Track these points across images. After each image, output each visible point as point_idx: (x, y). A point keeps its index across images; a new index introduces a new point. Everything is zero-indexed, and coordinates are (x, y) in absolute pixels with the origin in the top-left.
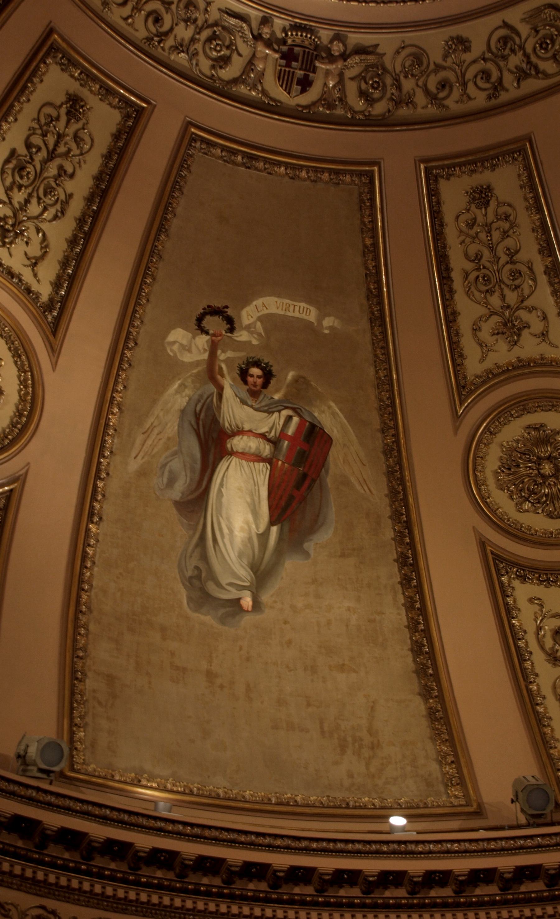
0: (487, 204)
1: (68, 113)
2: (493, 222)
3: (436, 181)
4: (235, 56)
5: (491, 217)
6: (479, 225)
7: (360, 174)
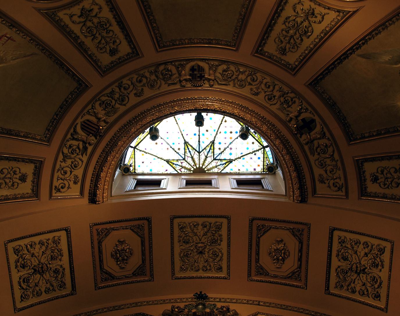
0: (110, 50)
1: (285, 49)
2: (106, 45)
3: (133, 52)
4: (221, 72)
5: (108, 47)
6: (111, 43)
7: (164, 46)
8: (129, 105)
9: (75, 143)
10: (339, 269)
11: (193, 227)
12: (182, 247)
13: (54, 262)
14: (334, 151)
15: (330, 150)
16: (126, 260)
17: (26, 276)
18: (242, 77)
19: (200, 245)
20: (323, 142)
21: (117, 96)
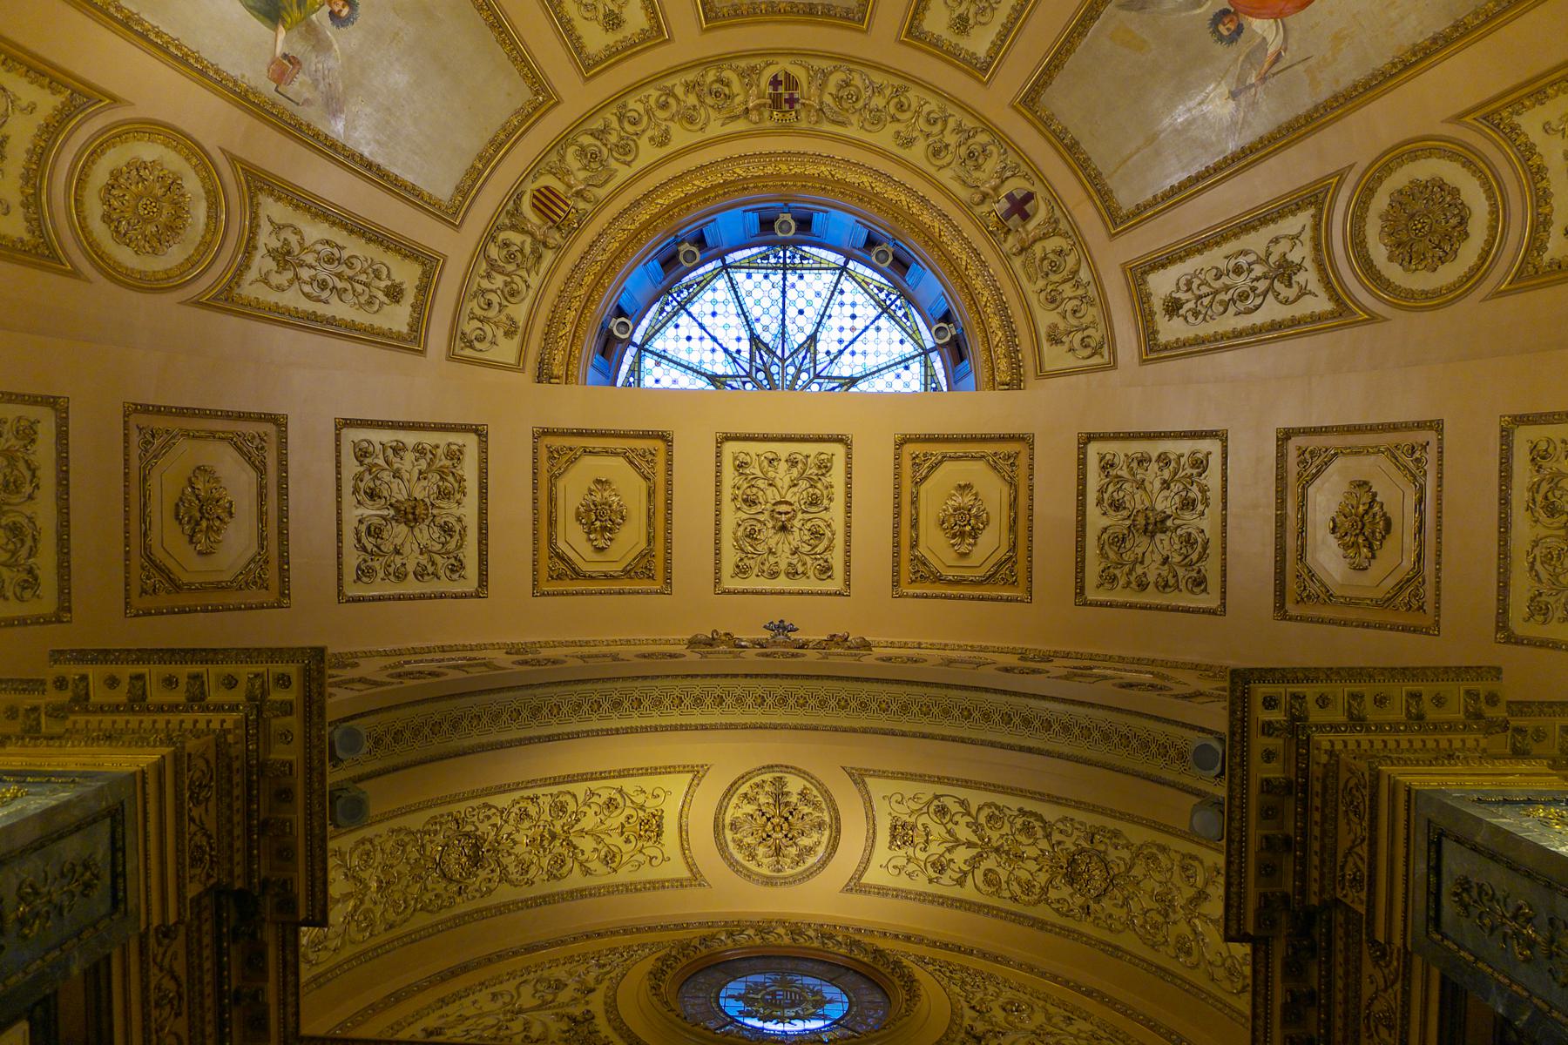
8: (638, 165)
9: (515, 237)
10: (1105, 536)
11: (766, 463)
12: (740, 514)
13: (444, 504)
14: (1079, 262)
15: (1071, 261)
16: (610, 531)
17: (377, 521)
18: (878, 101)
19: (783, 508)
20: (1054, 243)
21: (613, 138)
